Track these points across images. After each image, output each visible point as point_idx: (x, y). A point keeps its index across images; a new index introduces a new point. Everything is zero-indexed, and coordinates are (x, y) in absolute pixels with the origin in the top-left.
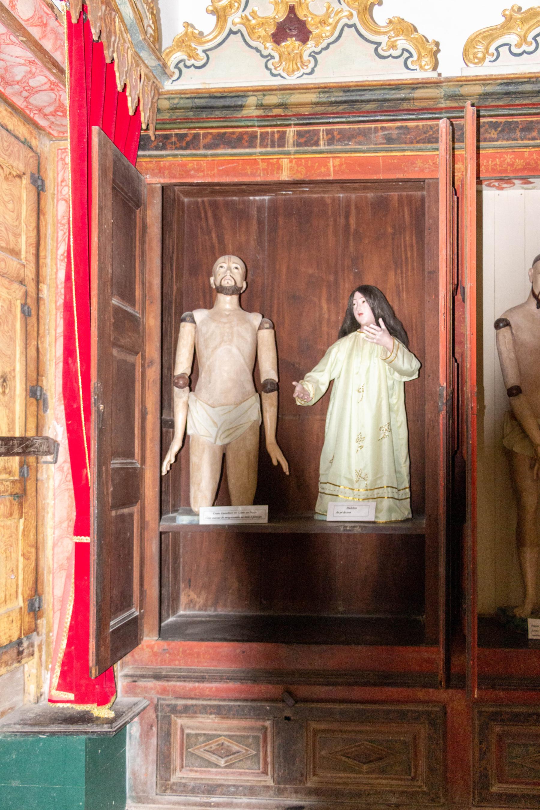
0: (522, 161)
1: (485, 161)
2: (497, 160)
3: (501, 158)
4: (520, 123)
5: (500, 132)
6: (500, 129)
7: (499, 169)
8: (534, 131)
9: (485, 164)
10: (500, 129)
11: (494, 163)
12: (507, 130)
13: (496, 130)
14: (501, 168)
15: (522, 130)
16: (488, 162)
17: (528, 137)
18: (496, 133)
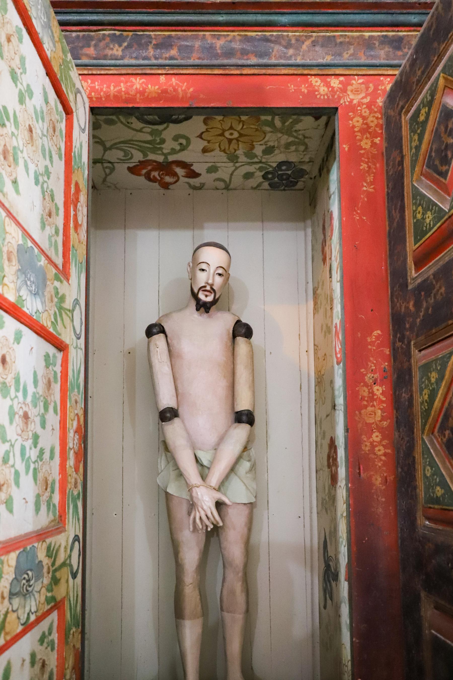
0: (157, 87)
1: (105, 86)
2: (122, 84)
3: (126, 82)
4: (153, 37)
5: (126, 48)
6: (125, 44)
7: (124, 98)
8: (173, 49)
9: (104, 90)
10: (125, 44)
11: (117, 88)
12: (136, 46)
13: (120, 46)
14: (127, 96)
15: (157, 46)
16: (109, 87)
17: (164, 56)
18: (120, 49)
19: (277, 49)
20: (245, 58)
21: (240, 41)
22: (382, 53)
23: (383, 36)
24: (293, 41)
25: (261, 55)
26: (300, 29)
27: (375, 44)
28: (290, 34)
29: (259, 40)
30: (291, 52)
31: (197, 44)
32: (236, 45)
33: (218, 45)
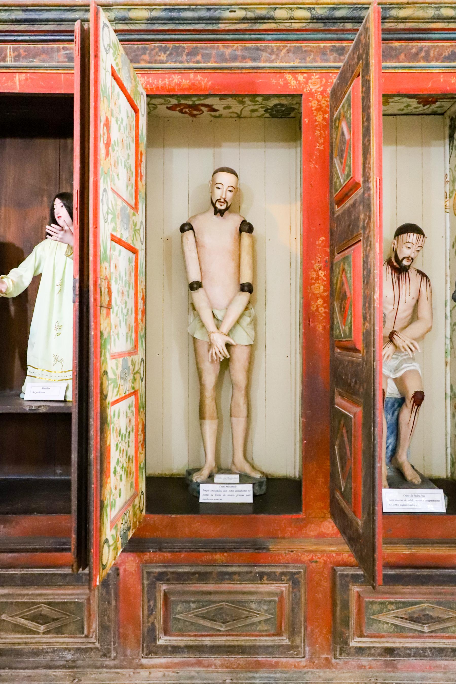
0: (188, 81)
1: (156, 80)
2: (166, 80)
3: (169, 78)
4: (186, 47)
5: (169, 55)
6: (168, 52)
7: (167, 88)
8: (198, 56)
9: (155, 83)
10: (168, 52)
11: (163, 82)
12: (175, 54)
13: (165, 53)
14: (170, 87)
15: (188, 54)
16: (158, 81)
17: (193, 60)
18: (165, 56)
19: (264, 55)
20: (244, 61)
21: (241, 50)
22: (332, 58)
23: (332, 46)
24: (275, 50)
25: (254, 60)
26: (279, 42)
27: (327, 51)
28: (273, 45)
29: (253, 49)
30: (273, 57)
31: (214, 52)
32: (239, 53)
33: (227, 53)
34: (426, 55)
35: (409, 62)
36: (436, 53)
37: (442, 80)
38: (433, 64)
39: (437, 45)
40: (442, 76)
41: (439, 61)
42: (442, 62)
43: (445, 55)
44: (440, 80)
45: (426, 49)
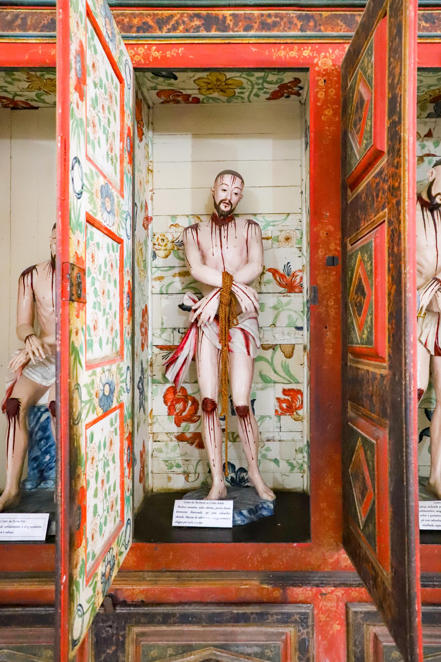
34: (22, 22)
35: (3, 31)
36: (34, 21)
37: (40, 52)
38: (30, 33)
39: (36, 12)
40: (40, 47)
41: (37, 30)
42: (41, 31)
43: (44, 24)
44: (38, 52)
45: (22, 16)
